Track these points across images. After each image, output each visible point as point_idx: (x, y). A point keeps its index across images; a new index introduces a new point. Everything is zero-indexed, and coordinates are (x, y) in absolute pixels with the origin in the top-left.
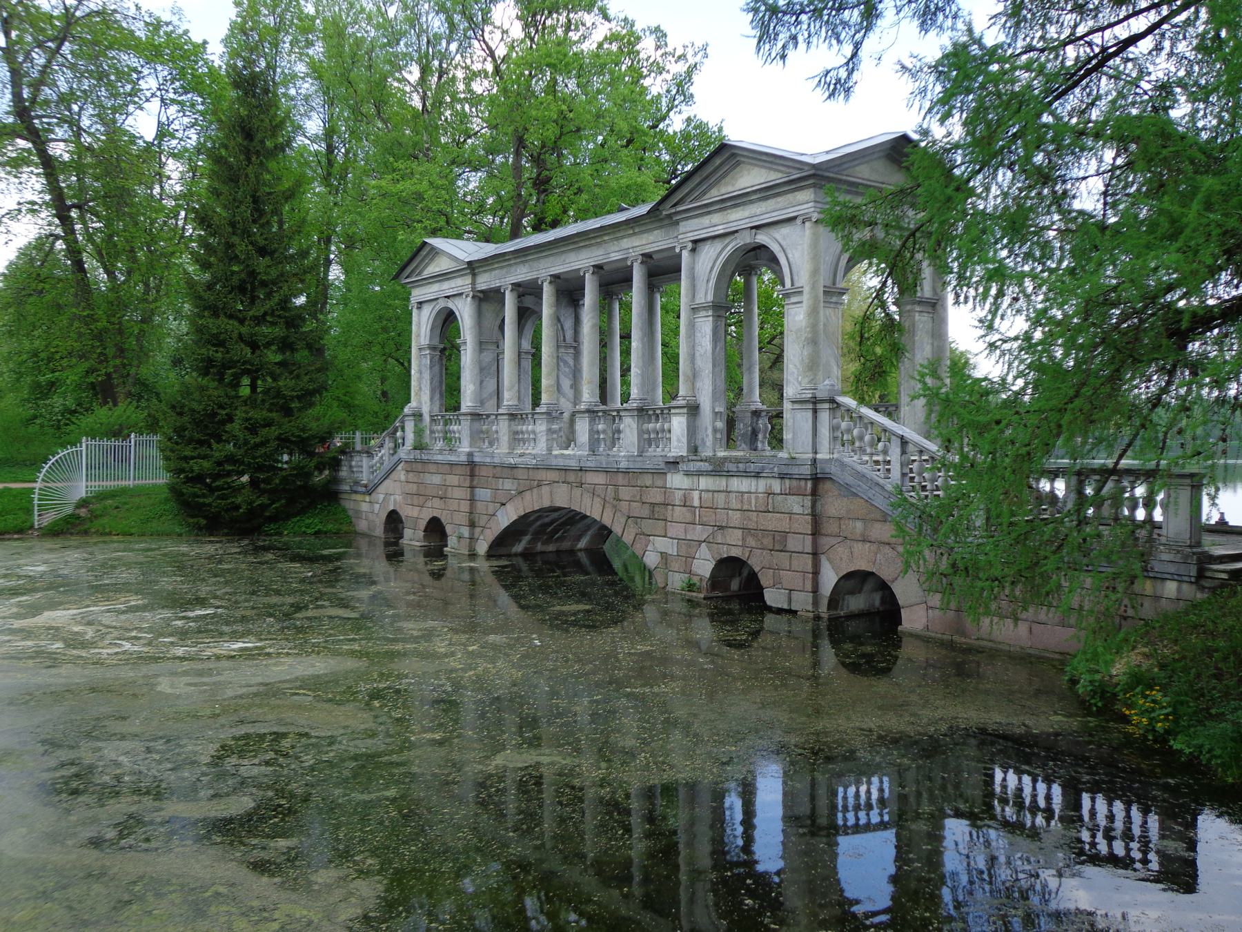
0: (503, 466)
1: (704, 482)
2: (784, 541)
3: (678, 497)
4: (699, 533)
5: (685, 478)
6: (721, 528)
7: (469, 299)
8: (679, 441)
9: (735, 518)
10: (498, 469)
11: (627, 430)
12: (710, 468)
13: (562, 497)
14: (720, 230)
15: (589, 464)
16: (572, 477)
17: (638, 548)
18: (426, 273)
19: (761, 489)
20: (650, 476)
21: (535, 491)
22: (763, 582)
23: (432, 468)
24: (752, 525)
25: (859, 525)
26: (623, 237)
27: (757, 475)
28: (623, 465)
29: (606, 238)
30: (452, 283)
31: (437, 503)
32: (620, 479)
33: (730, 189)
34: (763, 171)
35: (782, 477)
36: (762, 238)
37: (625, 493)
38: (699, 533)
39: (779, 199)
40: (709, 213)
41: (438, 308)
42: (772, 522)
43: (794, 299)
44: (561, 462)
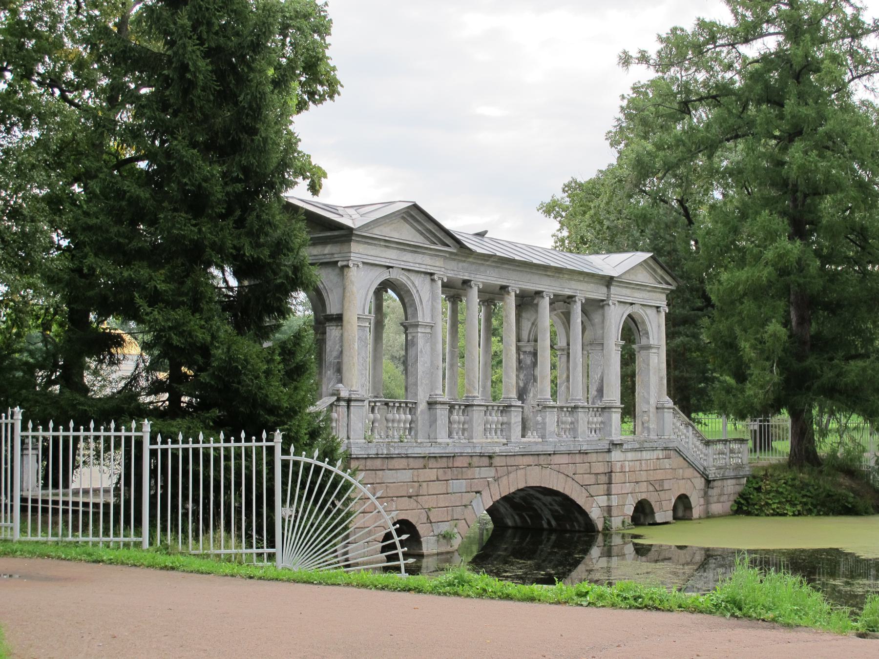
0: (481, 455)
1: (630, 456)
2: (662, 486)
3: (618, 466)
4: (628, 488)
5: (622, 454)
6: (637, 482)
7: (440, 283)
8: (616, 429)
9: (643, 476)
10: (475, 459)
11: (581, 422)
12: (637, 446)
13: (536, 478)
14: (630, 300)
15: (562, 449)
16: (542, 460)
17: (586, 507)
18: (377, 232)
19: (655, 457)
20: (595, 455)
21: (512, 476)
22: (655, 510)
23: (395, 463)
24: (651, 478)
25: (681, 471)
26: (575, 280)
27: (656, 449)
28: (584, 448)
29: (566, 276)
30: (419, 258)
31: (405, 503)
32: (578, 458)
33: (634, 278)
34: (648, 276)
35: (666, 449)
36: (641, 312)
37: (581, 468)
38: (628, 488)
39: (654, 294)
40: (627, 287)
41: (385, 275)
42: (659, 475)
43: (654, 351)
44: (539, 448)
